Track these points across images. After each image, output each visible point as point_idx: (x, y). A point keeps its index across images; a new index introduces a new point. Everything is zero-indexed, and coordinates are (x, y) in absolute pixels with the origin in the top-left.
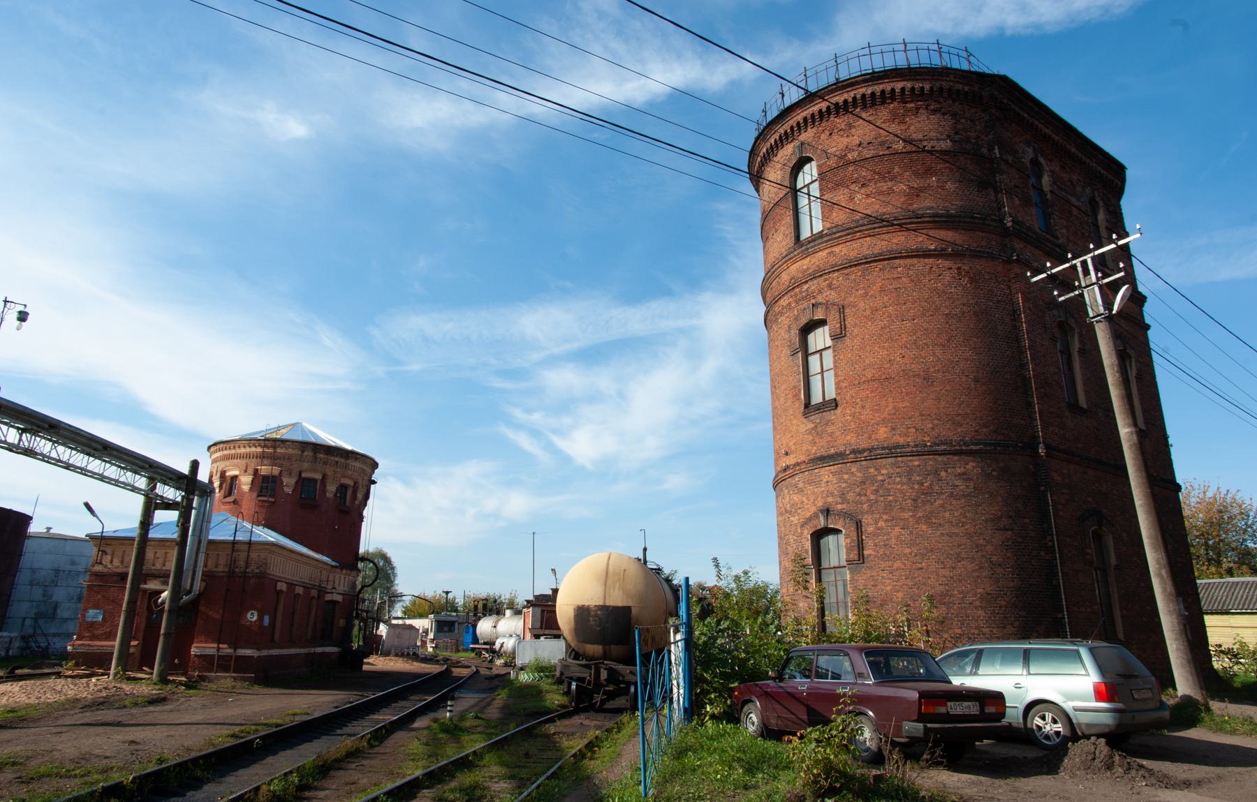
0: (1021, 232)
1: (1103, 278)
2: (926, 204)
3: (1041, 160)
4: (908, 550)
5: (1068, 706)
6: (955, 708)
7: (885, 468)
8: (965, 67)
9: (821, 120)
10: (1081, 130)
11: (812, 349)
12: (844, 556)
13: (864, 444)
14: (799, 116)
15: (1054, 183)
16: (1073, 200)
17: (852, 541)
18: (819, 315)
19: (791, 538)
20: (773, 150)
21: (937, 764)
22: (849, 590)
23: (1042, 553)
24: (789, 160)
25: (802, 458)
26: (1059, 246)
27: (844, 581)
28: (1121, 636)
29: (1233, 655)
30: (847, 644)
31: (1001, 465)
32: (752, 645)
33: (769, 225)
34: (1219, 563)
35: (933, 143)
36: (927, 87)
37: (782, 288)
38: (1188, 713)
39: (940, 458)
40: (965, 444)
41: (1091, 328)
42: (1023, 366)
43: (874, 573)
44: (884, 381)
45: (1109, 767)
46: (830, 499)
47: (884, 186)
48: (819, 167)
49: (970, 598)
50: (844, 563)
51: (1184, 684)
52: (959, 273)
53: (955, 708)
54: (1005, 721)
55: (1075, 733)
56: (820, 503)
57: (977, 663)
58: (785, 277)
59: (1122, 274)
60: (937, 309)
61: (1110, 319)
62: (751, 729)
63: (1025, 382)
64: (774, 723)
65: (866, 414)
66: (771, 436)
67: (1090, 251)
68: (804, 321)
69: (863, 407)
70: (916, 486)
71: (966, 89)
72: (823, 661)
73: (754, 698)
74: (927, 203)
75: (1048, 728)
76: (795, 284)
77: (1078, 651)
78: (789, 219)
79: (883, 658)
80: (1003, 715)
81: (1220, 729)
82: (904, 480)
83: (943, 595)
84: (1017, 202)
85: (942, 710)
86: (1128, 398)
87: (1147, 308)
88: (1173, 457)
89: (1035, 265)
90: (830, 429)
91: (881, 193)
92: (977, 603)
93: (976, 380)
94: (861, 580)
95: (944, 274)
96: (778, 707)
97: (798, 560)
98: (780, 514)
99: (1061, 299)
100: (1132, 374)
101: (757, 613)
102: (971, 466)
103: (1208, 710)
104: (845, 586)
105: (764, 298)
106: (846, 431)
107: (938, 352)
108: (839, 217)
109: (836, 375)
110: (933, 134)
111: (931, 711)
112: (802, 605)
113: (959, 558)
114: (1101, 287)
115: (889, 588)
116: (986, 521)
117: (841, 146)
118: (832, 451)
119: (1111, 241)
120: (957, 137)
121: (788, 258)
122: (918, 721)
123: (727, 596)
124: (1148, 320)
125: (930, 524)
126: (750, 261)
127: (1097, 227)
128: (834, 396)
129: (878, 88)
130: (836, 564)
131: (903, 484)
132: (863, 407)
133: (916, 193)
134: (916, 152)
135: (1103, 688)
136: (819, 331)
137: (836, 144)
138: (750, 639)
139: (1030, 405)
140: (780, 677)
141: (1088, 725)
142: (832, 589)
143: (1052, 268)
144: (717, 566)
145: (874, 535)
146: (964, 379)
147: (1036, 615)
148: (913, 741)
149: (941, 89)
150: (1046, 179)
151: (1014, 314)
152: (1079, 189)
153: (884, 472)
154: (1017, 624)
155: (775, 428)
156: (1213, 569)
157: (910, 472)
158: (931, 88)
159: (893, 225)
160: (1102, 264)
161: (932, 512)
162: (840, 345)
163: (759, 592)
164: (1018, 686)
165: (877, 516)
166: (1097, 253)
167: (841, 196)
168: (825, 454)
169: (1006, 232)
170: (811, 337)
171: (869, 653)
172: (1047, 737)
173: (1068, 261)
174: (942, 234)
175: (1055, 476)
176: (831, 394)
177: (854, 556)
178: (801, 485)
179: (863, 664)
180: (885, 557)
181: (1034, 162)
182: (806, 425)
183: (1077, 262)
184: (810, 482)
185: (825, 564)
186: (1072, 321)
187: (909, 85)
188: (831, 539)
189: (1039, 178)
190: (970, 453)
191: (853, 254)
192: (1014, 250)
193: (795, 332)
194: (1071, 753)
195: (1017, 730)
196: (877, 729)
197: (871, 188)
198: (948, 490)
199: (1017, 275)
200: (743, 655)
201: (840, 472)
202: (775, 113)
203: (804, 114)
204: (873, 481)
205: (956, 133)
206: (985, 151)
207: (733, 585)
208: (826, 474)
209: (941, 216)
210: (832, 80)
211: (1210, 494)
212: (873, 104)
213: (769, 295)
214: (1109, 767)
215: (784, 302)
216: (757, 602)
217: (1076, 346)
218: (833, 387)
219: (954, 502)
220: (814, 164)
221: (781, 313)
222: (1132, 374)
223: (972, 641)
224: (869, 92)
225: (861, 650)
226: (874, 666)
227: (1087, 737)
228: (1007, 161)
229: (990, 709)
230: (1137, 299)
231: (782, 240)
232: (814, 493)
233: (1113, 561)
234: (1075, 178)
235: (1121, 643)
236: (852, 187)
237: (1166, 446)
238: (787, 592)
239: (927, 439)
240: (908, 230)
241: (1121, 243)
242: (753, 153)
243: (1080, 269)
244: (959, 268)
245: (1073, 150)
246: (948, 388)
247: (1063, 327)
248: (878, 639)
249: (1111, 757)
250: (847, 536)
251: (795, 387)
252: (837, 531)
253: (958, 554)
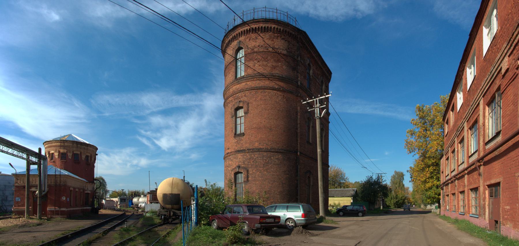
2: (276, 72)
5: (295, 219)
6: (268, 220)
7: (256, 155)
8: (294, 25)
11: (238, 116)
12: (243, 180)
13: (251, 148)
14: (240, 30)
15: (313, 73)
18: (241, 105)
21: (263, 234)
25: (233, 150)
29: (333, 206)
32: (215, 204)
35: (281, 51)
36: (282, 29)
38: (321, 220)
41: (315, 120)
42: (297, 129)
45: (302, 233)
47: (265, 63)
48: (245, 52)
51: (321, 213)
55: (296, 225)
57: (275, 209)
58: (231, 90)
61: (320, 118)
62: (214, 227)
64: (221, 225)
68: (236, 106)
71: (294, 33)
72: (235, 209)
74: (277, 72)
76: (234, 93)
79: (251, 208)
80: (280, 222)
81: (326, 223)
85: (265, 221)
86: (321, 141)
87: (330, 117)
90: (242, 142)
91: (263, 65)
97: (230, 180)
100: (324, 135)
101: (217, 196)
102: (280, 156)
108: (250, 71)
112: (230, 193)
117: (253, 45)
121: (232, 84)
123: (209, 191)
129: (267, 25)
133: (274, 67)
136: (241, 110)
137: (252, 44)
139: (297, 140)
140: (223, 213)
142: (239, 189)
144: (206, 182)
147: (291, 198)
148: (258, 229)
149: (286, 31)
150: (311, 71)
152: (319, 77)
160: (321, 102)
162: (246, 116)
163: (218, 189)
167: (251, 64)
169: (298, 86)
170: (238, 112)
171: (248, 206)
172: (290, 227)
173: (312, 99)
176: (243, 131)
179: (246, 209)
181: (309, 65)
182: (233, 140)
184: (235, 158)
185: (237, 182)
187: (276, 27)
189: (310, 71)
191: (253, 85)
193: (233, 110)
196: (248, 226)
197: (260, 63)
201: (244, 155)
202: (232, 27)
203: (241, 30)
206: (296, 57)
208: (239, 156)
209: (280, 77)
210: (252, 18)
215: (230, 99)
216: (218, 192)
217: (311, 125)
220: (243, 50)
221: (229, 103)
222: (324, 135)
224: (264, 26)
225: (246, 206)
226: (249, 210)
229: (277, 220)
230: (328, 114)
231: (231, 77)
233: (312, 184)
235: (310, 204)
236: (255, 61)
237: (328, 155)
238: (226, 190)
247: (309, 119)
248: (250, 203)
252: (241, 173)
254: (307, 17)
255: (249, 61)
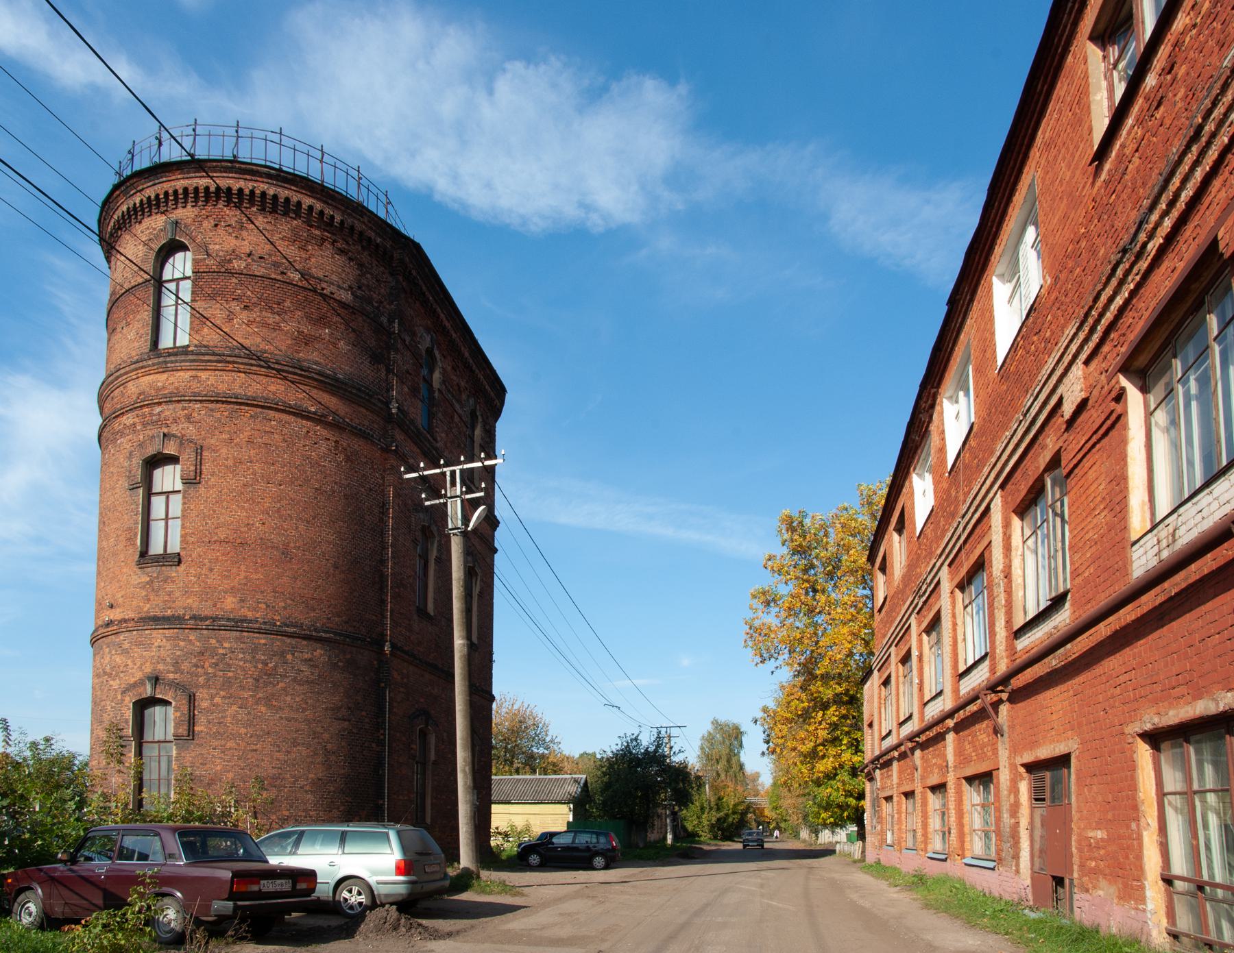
0: (402, 422)
1: (467, 493)
2: (313, 357)
3: (436, 352)
4: (243, 731)
5: (372, 880)
6: (268, 886)
7: (228, 642)
8: (382, 214)
9: (207, 201)
10: (477, 336)
11: (157, 488)
12: (171, 730)
13: (207, 613)
14: (180, 182)
15: (444, 382)
16: (457, 406)
17: (183, 714)
18: (171, 449)
19: (109, 705)
20: (136, 214)
21: (242, 939)
22: (174, 766)
23: (374, 745)
24: (157, 237)
25: (131, 615)
26: (436, 449)
27: (170, 757)
28: (428, 820)
29: (506, 835)
30: (164, 824)
31: (348, 656)
32: (42, 824)
33: (118, 313)
34: (512, 763)
35: (333, 289)
36: (338, 218)
37: (127, 401)
38: (465, 881)
39: (288, 640)
40: (315, 630)
41: (448, 536)
42: (383, 562)
43: (204, 751)
44: (238, 545)
45: (395, 928)
46: (161, 667)
47: (272, 319)
48: (195, 262)
49: (301, 783)
50: (170, 737)
51: (466, 859)
52: (336, 448)
53: (268, 886)
54: (314, 896)
55: (374, 903)
56: (148, 669)
57: (297, 844)
58: (132, 389)
59: (482, 494)
60: (307, 480)
61: (465, 534)
62: (26, 920)
63: (383, 578)
64: (58, 911)
65: (214, 579)
66: (94, 581)
67: (460, 463)
68: (150, 451)
69: (211, 570)
70: (260, 666)
71: (379, 240)
72: (129, 842)
73: (35, 885)
74: (315, 356)
75: (353, 899)
76: (142, 403)
77: (387, 834)
78: (146, 315)
79: (199, 839)
80: (313, 890)
81: (483, 892)
82: (248, 657)
83: (274, 778)
84: (406, 389)
85: (255, 888)
86: (468, 611)
87: (498, 534)
88: (494, 672)
89: (411, 461)
90: (169, 587)
91: (265, 325)
92: (308, 788)
93: (336, 567)
94: (188, 757)
95: (317, 445)
96: (65, 892)
97: (115, 730)
98: (97, 675)
99: (427, 503)
100: (476, 591)
101: (58, 787)
102: (319, 652)
103: (478, 877)
104: (169, 762)
105: (101, 408)
106: (187, 593)
107: (301, 527)
108: (211, 337)
109: (183, 527)
110: (334, 278)
111: (243, 889)
112: (115, 780)
113: (295, 743)
114: (462, 501)
115: (219, 768)
116: (326, 709)
117: (227, 247)
118: (169, 613)
119: (481, 460)
120: (359, 293)
121: (138, 365)
122: (228, 899)
123: (17, 765)
124: (497, 545)
125: (270, 707)
126: (90, 355)
127: (473, 441)
128: (178, 550)
129: (283, 193)
130: (162, 738)
131: (245, 662)
132: (211, 570)
133: (305, 340)
134: (311, 291)
135: (402, 865)
136: (169, 469)
137: (222, 242)
138: (39, 817)
139: (383, 602)
140: (73, 860)
141: (386, 895)
142: (154, 765)
143: (425, 469)
144: (6, 729)
145: (208, 710)
146: (324, 562)
147: (357, 801)
148: (222, 919)
149: (352, 228)
150: (437, 376)
151: (383, 506)
152: (464, 397)
153: (226, 645)
154: (342, 808)
155: (99, 573)
156: (507, 768)
157: (255, 650)
158: (342, 222)
159: (269, 367)
160: (469, 480)
161: (273, 695)
162: (191, 492)
163: (65, 762)
164: (332, 864)
165: (213, 691)
166: (466, 466)
167: (216, 311)
168: (159, 614)
169: (389, 418)
170: (157, 473)
171: (183, 833)
172: (351, 907)
173: (439, 466)
174: (326, 398)
175: (395, 674)
176: (175, 546)
177: (183, 730)
178: (126, 645)
179: (174, 844)
180: (218, 735)
181: (429, 352)
182: (140, 577)
183: (447, 470)
184: (139, 644)
185: (148, 736)
186: (434, 528)
187: (318, 206)
188: (158, 710)
189: (431, 371)
190: (319, 640)
191: (222, 388)
192: (394, 440)
193: (137, 462)
194: (367, 920)
195: (326, 903)
196: (184, 908)
197: (255, 314)
198: (293, 674)
199: (393, 468)
200: (27, 836)
201: (177, 638)
202: (146, 164)
203: (186, 183)
204: (214, 654)
205: (359, 288)
206: (384, 320)
207: (28, 753)
208: (159, 638)
209: (328, 377)
210: (228, 155)
211: (516, 707)
212: (274, 211)
213: (108, 405)
214: (395, 928)
215: (128, 419)
216: (57, 774)
217: (434, 554)
218: (178, 539)
219: (297, 687)
220: (189, 254)
221: (122, 434)
222: (476, 591)
223: (298, 822)
224: (271, 192)
225: (174, 830)
226: (189, 848)
227: (383, 905)
228: (404, 340)
229: (302, 886)
230: (491, 521)
231: (133, 340)
232: (141, 656)
233: (432, 756)
234: (463, 384)
235: (428, 828)
236: (234, 304)
237: (491, 661)
238: (99, 764)
239: (277, 618)
240: (285, 378)
241: (487, 463)
242: (108, 204)
243: (448, 478)
244: (336, 442)
245: (467, 354)
246: (306, 567)
247: (427, 533)
248: (200, 819)
249: (399, 920)
250: (177, 709)
251: (130, 529)
252: (166, 703)
253: (295, 739)
254: (424, 199)
255: (212, 297)
